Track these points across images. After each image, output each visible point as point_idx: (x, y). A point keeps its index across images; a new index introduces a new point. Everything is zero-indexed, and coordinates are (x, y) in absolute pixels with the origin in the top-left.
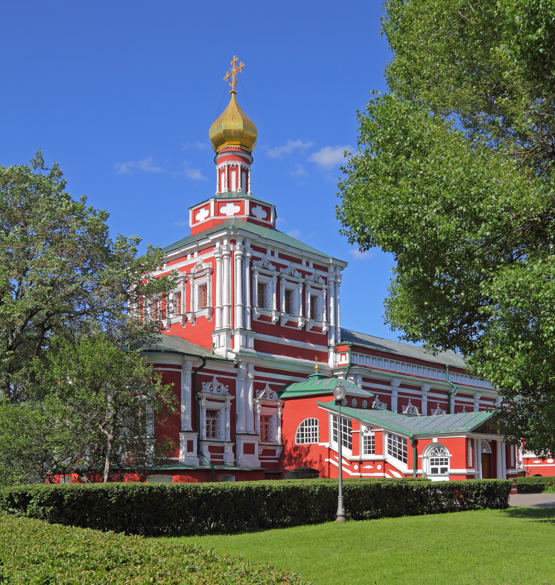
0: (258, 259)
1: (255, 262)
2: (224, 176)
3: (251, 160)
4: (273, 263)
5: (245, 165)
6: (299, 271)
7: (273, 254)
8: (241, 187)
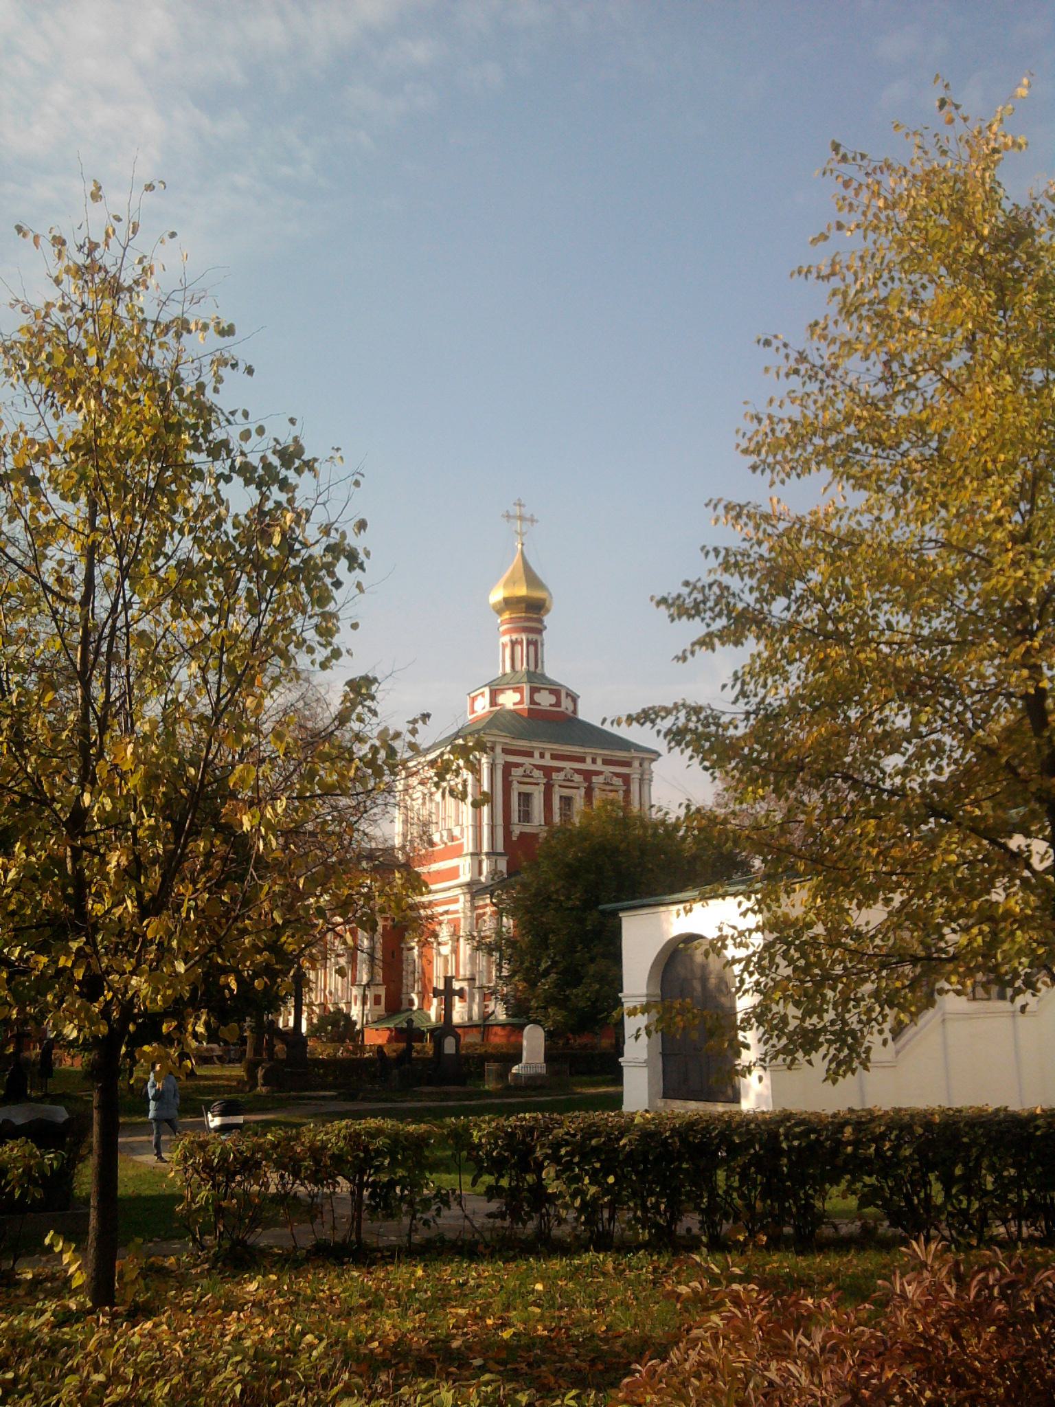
0: (518, 765)
1: (515, 771)
2: (508, 651)
5: (533, 637)
6: (578, 771)
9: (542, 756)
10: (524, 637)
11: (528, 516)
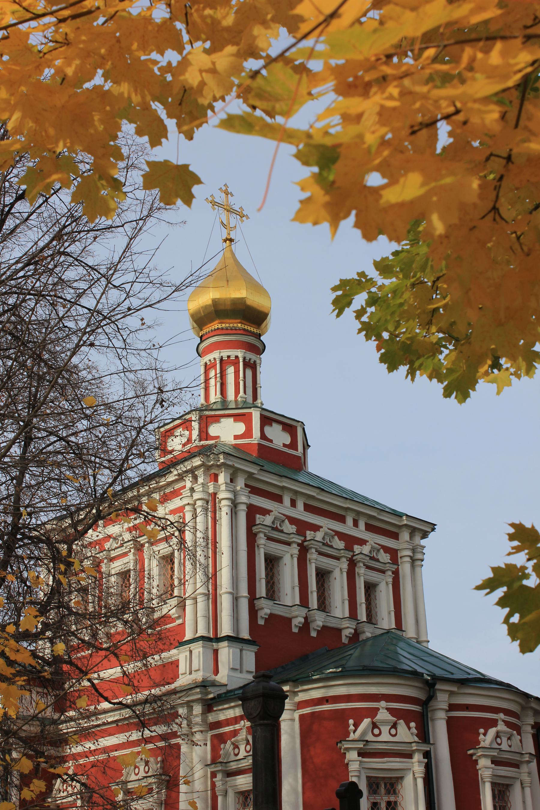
0: (266, 512)
1: (259, 518)
3: (261, 348)
4: (293, 521)
5: (250, 356)
7: (293, 503)
8: (245, 392)
9: (293, 503)
10: (240, 353)
11: (236, 208)
